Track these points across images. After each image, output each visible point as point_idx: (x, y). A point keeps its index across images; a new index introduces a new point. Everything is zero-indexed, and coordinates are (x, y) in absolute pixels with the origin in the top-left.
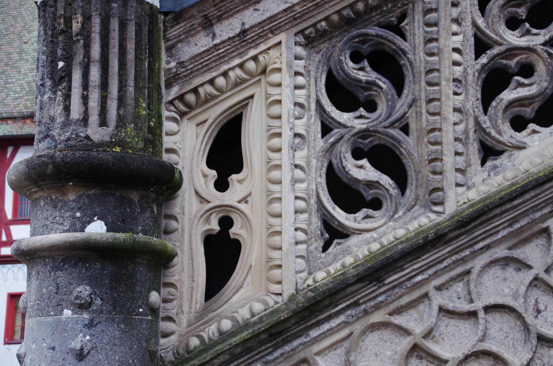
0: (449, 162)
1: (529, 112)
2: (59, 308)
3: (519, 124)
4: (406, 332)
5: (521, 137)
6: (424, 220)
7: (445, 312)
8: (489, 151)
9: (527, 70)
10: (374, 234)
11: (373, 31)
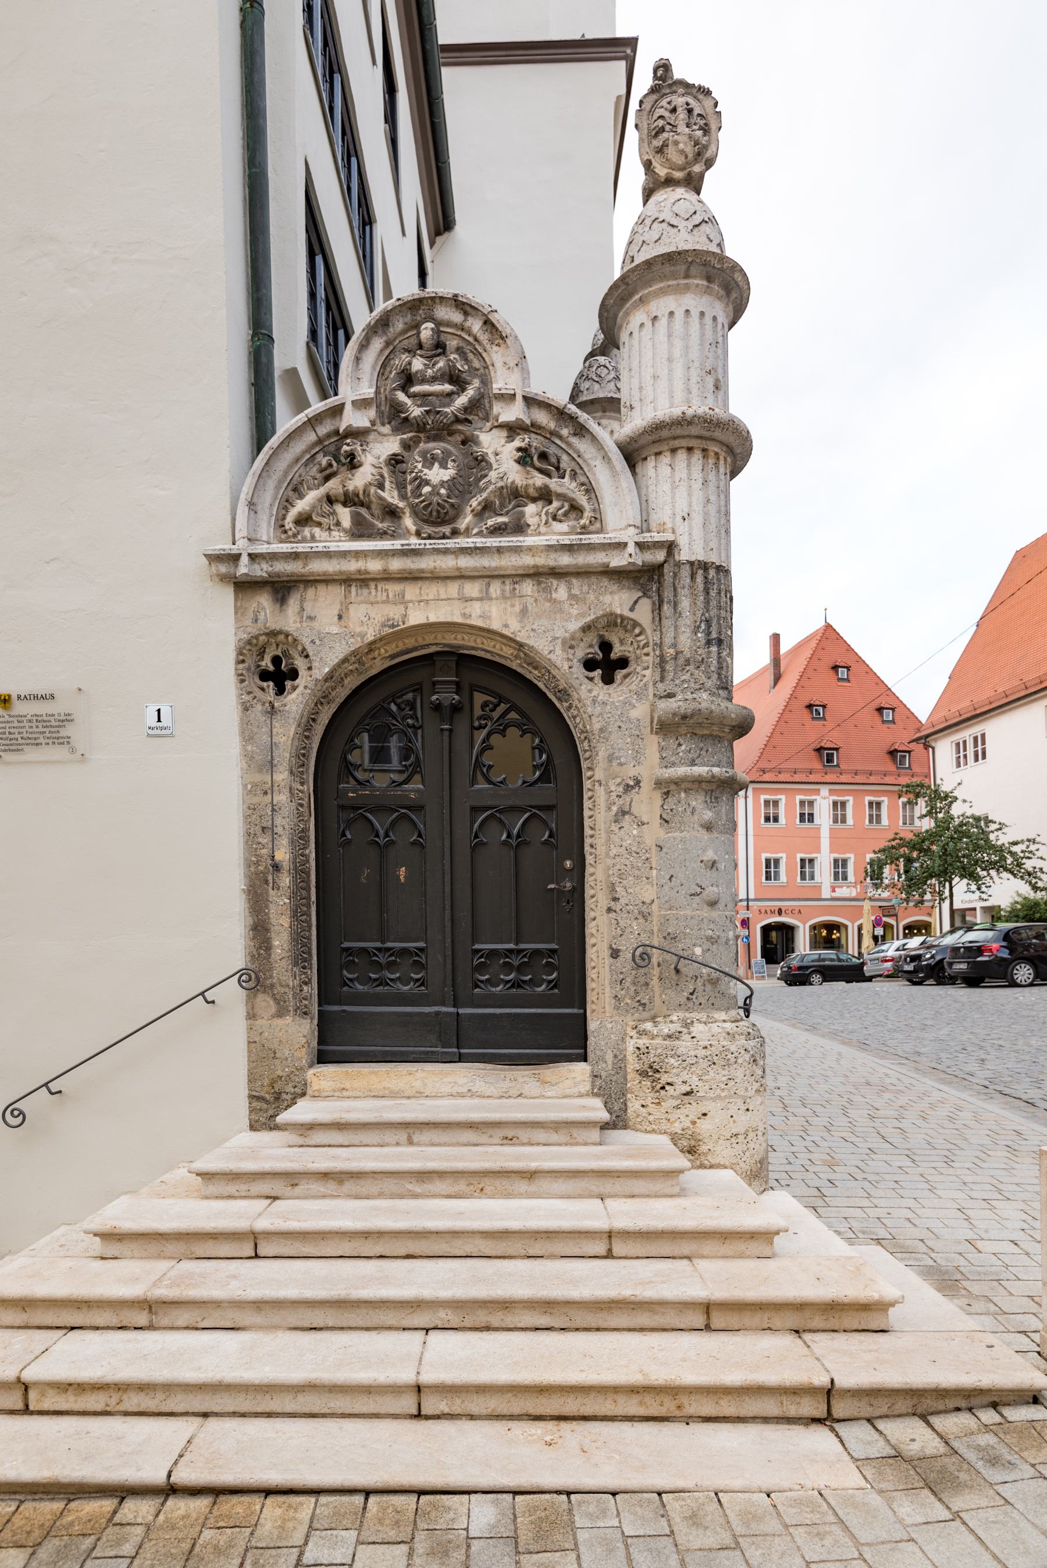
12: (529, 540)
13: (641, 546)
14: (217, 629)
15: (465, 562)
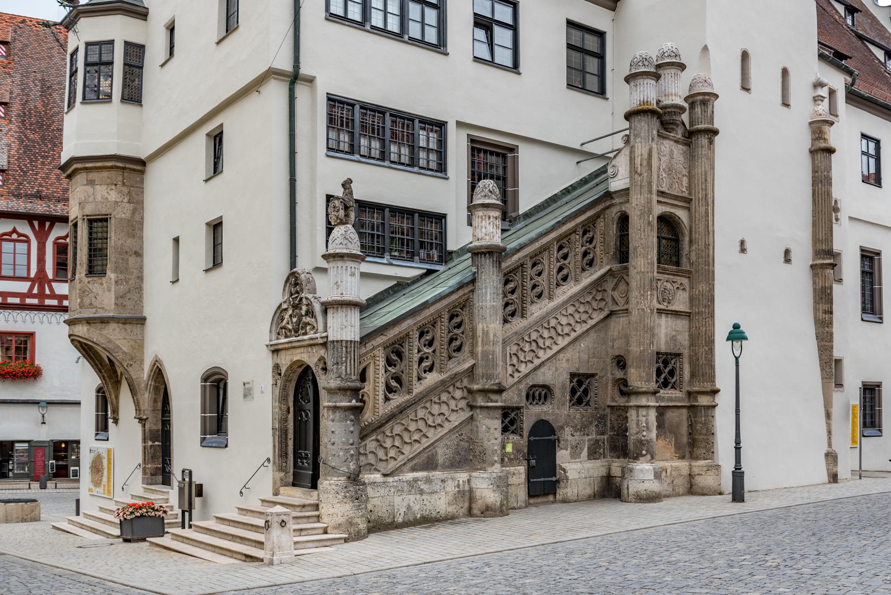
2: (346, 420)
5: (425, 375)
6: (407, 397)
8: (419, 379)
10: (397, 400)
12: (306, 337)
13: (322, 338)
14: (267, 361)
15: (299, 344)
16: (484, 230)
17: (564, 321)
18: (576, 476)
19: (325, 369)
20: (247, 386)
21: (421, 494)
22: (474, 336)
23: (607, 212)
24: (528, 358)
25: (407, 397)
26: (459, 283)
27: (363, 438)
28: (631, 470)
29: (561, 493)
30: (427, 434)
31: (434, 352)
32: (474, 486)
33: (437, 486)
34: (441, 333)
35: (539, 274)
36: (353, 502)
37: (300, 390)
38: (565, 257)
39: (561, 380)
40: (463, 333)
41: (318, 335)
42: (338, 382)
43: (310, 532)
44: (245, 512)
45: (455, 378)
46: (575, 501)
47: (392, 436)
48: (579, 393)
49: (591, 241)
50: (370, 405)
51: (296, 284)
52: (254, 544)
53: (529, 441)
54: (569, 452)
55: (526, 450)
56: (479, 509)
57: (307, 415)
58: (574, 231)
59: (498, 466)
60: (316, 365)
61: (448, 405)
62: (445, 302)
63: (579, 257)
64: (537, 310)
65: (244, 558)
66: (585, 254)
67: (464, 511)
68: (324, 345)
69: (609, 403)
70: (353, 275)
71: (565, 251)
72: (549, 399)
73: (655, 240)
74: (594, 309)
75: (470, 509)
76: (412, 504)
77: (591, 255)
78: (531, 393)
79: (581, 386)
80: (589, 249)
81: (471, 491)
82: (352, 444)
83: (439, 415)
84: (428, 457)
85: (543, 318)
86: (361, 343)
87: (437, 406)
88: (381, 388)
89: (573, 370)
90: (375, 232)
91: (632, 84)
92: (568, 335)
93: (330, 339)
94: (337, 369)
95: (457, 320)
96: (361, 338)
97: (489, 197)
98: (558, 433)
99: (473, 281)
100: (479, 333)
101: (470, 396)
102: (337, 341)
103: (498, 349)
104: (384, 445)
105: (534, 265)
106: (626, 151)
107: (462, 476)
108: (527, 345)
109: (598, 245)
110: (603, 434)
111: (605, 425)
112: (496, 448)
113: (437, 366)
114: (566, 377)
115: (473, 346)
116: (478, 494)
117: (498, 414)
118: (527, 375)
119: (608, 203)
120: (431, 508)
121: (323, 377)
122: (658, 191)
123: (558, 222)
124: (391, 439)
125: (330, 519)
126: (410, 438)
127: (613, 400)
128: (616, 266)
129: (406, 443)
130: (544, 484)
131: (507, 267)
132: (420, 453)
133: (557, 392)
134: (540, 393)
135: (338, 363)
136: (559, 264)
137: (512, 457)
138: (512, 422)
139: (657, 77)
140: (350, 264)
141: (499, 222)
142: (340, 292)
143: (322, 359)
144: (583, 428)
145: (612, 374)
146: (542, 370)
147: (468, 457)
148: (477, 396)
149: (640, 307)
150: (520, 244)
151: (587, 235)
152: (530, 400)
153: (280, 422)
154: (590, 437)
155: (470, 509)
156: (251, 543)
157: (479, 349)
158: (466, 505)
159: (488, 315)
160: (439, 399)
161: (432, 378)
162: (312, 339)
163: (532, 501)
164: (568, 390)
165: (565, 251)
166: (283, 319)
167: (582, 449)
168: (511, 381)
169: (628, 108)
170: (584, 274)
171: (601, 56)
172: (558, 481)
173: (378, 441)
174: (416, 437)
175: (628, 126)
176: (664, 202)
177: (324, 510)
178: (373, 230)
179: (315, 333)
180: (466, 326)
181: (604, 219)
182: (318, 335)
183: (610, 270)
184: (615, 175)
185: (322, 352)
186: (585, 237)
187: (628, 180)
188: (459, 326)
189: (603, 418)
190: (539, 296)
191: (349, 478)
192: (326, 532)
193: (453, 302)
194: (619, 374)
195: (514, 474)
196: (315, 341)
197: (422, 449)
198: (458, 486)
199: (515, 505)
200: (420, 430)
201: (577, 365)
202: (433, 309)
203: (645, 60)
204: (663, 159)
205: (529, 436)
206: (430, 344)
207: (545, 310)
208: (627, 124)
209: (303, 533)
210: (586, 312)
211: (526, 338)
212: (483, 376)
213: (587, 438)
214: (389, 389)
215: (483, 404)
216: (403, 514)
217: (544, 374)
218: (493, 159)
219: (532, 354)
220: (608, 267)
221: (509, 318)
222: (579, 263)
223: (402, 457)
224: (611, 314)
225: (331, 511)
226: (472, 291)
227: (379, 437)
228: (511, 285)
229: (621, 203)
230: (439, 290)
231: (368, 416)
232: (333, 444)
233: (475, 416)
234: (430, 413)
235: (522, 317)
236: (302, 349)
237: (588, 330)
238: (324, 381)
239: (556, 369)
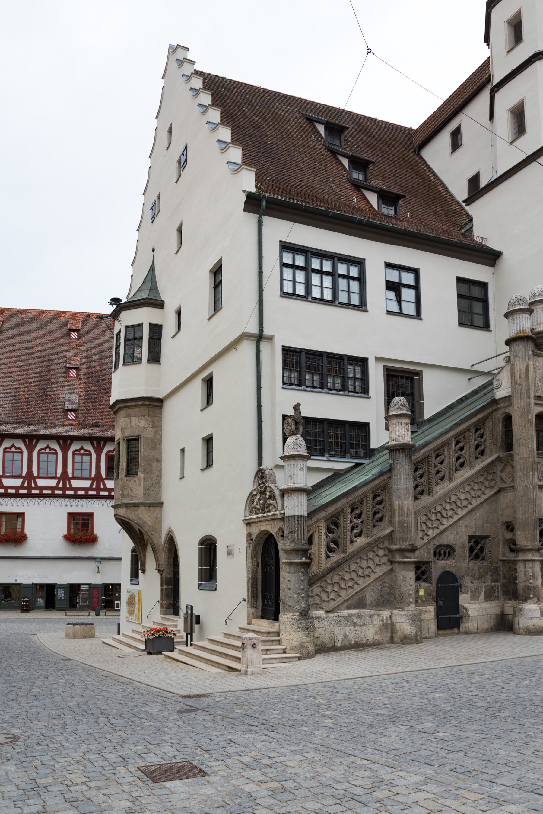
0: (348, 544)
1: (357, 535)
2: (299, 572)
3: (356, 537)
4: (340, 575)
6: (343, 555)
7: (346, 572)
8: (352, 542)
9: (357, 527)
10: (336, 557)
11: (335, 519)
12: (269, 514)
13: (280, 514)
16: (397, 433)
17: (462, 497)
18: (476, 614)
19: (283, 536)
20: (229, 548)
21: (355, 626)
22: (392, 510)
23: (494, 414)
24: (434, 525)
25: (343, 555)
26: (380, 472)
27: (311, 584)
28: (521, 610)
29: (464, 627)
30: (359, 582)
31: (362, 522)
32: (395, 621)
33: (366, 620)
34: (367, 508)
35: (442, 463)
36: (304, 631)
37: (266, 551)
38: (461, 449)
39: (461, 541)
40: (383, 508)
41: (278, 512)
42: (293, 545)
43: (274, 652)
44: (228, 636)
45: (379, 540)
46: (476, 633)
47: (332, 584)
48: (476, 551)
49: (482, 436)
50: (315, 561)
51: (262, 477)
52: (234, 659)
53: (437, 587)
54: (469, 595)
55: (435, 594)
56: (399, 638)
57: (271, 568)
58: (468, 430)
59: (413, 606)
60: (277, 533)
61: (373, 561)
62: (369, 486)
63: (473, 449)
64: (440, 490)
65: (227, 669)
66: (477, 446)
67: (387, 639)
68: (282, 519)
69: (501, 558)
70: (302, 469)
71: (461, 445)
72: (452, 556)
73: (534, 433)
74: (486, 487)
75: (392, 638)
76: (347, 633)
77: (482, 447)
78: (438, 551)
79: (477, 546)
80: (481, 442)
81: (392, 624)
82: (303, 590)
83: (367, 568)
84: (359, 599)
85: (445, 495)
86: (308, 517)
87: (365, 562)
88: (324, 549)
89: (471, 533)
90: (318, 439)
91: (510, 318)
92: (466, 507)
93: (286, 515)
94: (291, 536)
95: (378, 499)
96: (309, 514)
97: (401, 409)
98: (460, 581)
99: (390, 470)
100: (396, 508)
101: (390, 554)
102: (291, 516)
103: (411, 519)
104: (326, 590)
105: (437, 456)
106: (508, 368)
107: (386, 613)
108: (434, 516)
109: (488, 439)
110: (496, 581)
111: (499, 575)
112: (411, 592)
113: (364, 532)
114: (465, 539)
115: (392, 517)
116: (398, 626)
117: (412, 567)
118: (434, 538)
119: (494, 408)
120: (362, 637)
121: (282, 542)
122: (535, 396)
123: (455, 424)
124: (331, 586)
125: (288, 643)
126: (346, 585)
127: (504, 555)
128: (503, 454)
129: (342, 588)
130: (450, 619)
131: (416, 459)
132: (353, 596)
133: (458, 550)
134: (445, 551)
135: (292, 532)
136: (456, 455)
137: (424, 599)
138: (423, 573)
139: (530, 311)
140: (300, 462)
141: (409, 427)
142: (292, 482)
143: (281, 529)
144: (480, 577)
145: (503, 536)
146: (446, 534)
147: (390, 599)
148: (396, 554)
149: (524, 484)
150: (426, 442)
151: (479, 432)
152: (437, 556)
153: (252, 573)
154: (487, 584)
155: (392, 638)
156: (231, 658)
157: (397, 519)
158: (389, 635)
159: (402, 494)
160: (367, 556)
161: (361, 541)
162: (273, 515)
163: (440, 632)
164: (467, 548)
165: (461, 445)
166: (253, 502)
167: (480, 594)
168: (421, 542)
169: (507, 337)
170: (477, 461)
171: (485, 301)
172: (461, 618)
173: (321, 587)
174: (350, 584)
175: (508, 350)
176: (541, 404)
177: (284, 636)
178: (316, 437)
179: (276, 511)
180: (386, 503)
181: (492, 419)
182: (278, 512)
183: (498, 457)
184: (499, 387)
185: (281, 524)
186: (477, 433)
187: (510, 390)
188: (380, 503)
189: (496, 569)
190: (442, 479)
191: (301, 613)
192: (285, 652)
193: (376, 486)
194: (509, 536)
195: (426, 612)
196: (276, 517)
197: (354, 593)
198: (383, 620)
199: (427, 635)
200: (353, 579)
201: (474, 530)
202: (360, 492)
203: (520, 300)
204: (538, 372)
205: (437, 583)
206: (359, 516)
207: (447, 489)
208: (507, 348)
209: (269, 652)
210: (480, 489)
211: (433, 510)
212: (400, 539)
213: (484, 585)
214: (330, 549)
215: (400, 560)
216: (341, 640)
217: (447, 536)
218: (403, 382)
219: (438, 522)
220: (496, 455)
221: (419, 496)
222: (473, 453)
223: (339, 599)
224: (500, 490)
225: (289, 637)
226: (390, 477)
227: (323, 584)
228: (420, 472)
229: (505, 407)
230: (365, 478)
231: (314, 569)
232: (289, 589)
233: (394, 568)
234: (360, 566)
235: (429, 495)
236: (267, 523)
237: (481, 503)
238: (282, 545)
239: (457, 533)
